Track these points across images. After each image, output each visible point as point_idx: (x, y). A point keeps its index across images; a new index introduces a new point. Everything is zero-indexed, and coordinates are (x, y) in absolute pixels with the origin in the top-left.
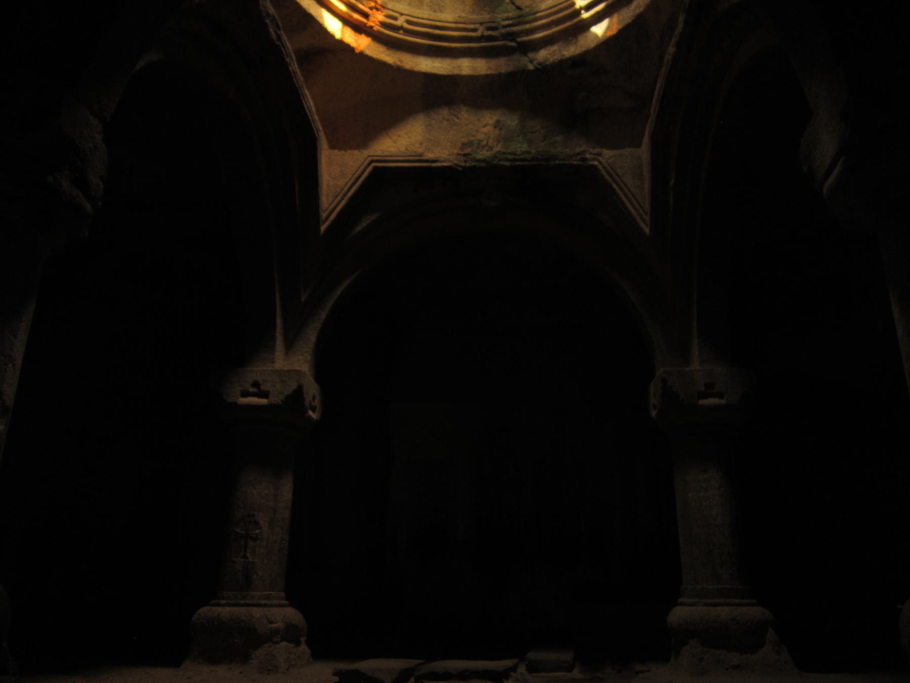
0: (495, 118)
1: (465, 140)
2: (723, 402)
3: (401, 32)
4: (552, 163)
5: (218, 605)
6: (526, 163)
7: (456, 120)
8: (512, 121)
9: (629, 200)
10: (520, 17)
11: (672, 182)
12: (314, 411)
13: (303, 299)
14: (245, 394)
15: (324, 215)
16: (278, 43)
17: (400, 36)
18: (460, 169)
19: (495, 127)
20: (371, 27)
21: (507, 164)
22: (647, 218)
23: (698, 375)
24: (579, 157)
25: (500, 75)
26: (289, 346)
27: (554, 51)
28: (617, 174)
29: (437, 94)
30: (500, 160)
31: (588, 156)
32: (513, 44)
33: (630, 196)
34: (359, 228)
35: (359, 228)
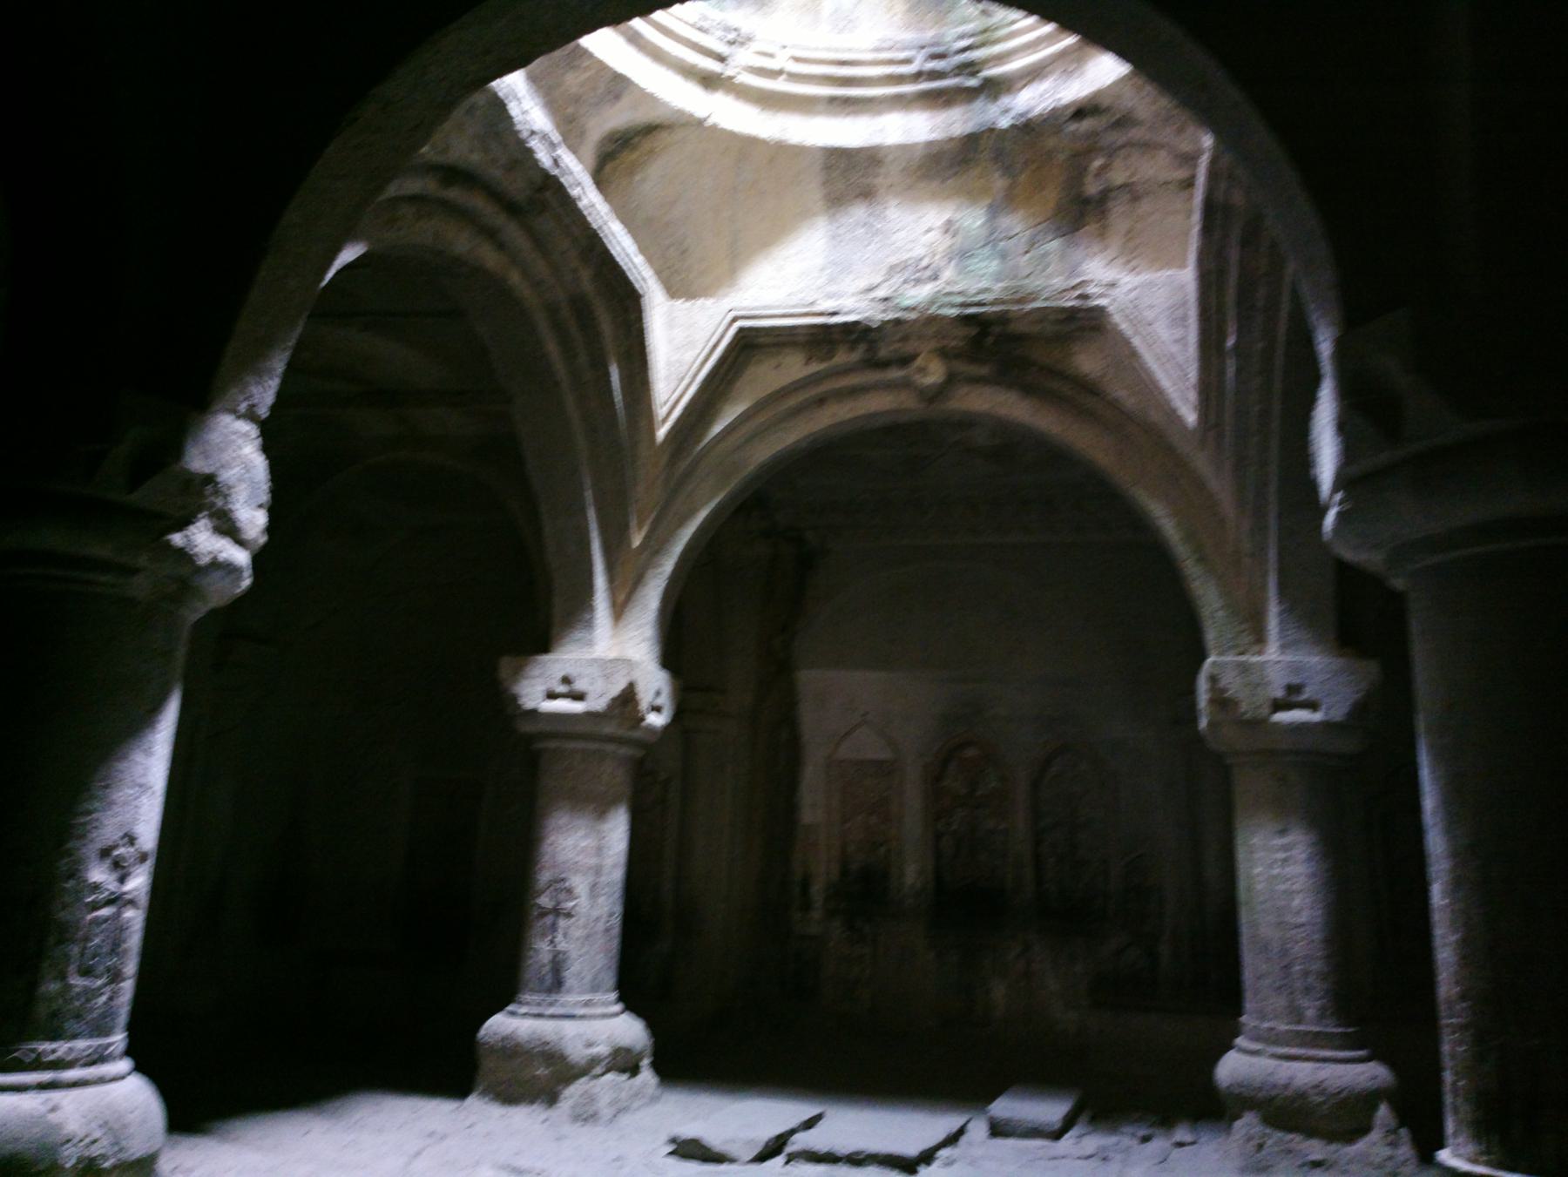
0: (946, 216)
1: (893, 260)
2: (1317, 717)
5: (513, 1014)
8: (973, 219)
10: (985, 31)
11: (1230, 342)
12: (657, 709)
13: (637, 541)
14: (552, 696)
15: (661, 412)
16: (555, 172)
17: (780, 85)
19: (946, 232)
20: (731, 78)
21: (953, 312)
22: (1193, 396)
23: (1273, 668)
24: (1078, 292)
25: (951, 139)
26: (619, 611)
27: (1046, 91)
29: (850, 178)
31: (1091, 290)
32: (973, 82)
34: (717, 429)
35: (717, 429)
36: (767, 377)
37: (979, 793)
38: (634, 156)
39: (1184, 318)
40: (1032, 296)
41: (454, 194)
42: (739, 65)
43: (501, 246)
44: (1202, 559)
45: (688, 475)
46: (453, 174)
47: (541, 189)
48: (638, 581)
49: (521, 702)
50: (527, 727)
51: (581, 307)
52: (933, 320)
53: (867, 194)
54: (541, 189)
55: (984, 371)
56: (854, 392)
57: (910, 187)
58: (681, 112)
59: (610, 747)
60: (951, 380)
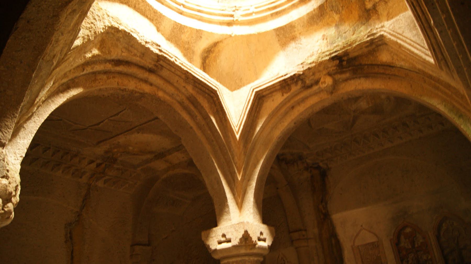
3: (254, 14)
4: (354, 45)
6: (339, 52)
7: (300, 45)
9: (413, 46)
11: (432, 22)
12: (264, 240)
14: (220, 243)
16: (160, 54)
17: (254, 16)
18: (302, 73)
20: (237, 20)
21: (327, 58)
22: (429, 53)
25: (314, 10)
26: (240, 205)
28: (398, 33)
29: (286, 35)
30: (322, 58)
33: (412, 43)
35: (258, 129)
36: (270, 105)
37: (416, 246)
38: (214, 55)
39: (415, 26)
40: (355, 41)
41: (120, 68)
42: (238, 16)
43: (151, 85)
44: (461, 116)
45: (253, 149)
46: (118, 62)
47: (158, 61)
48: (245, 193)
49: (211, 247)
50: (216, 257)
51: (193, 100)
52: (321, 64)
53: (294, 38)
54: (158, 61)
55: (348, 75)
56: (304, 100)
57: (307, 31)
58: (223, 35)
59: (247, 258)
60: (335, 83)
